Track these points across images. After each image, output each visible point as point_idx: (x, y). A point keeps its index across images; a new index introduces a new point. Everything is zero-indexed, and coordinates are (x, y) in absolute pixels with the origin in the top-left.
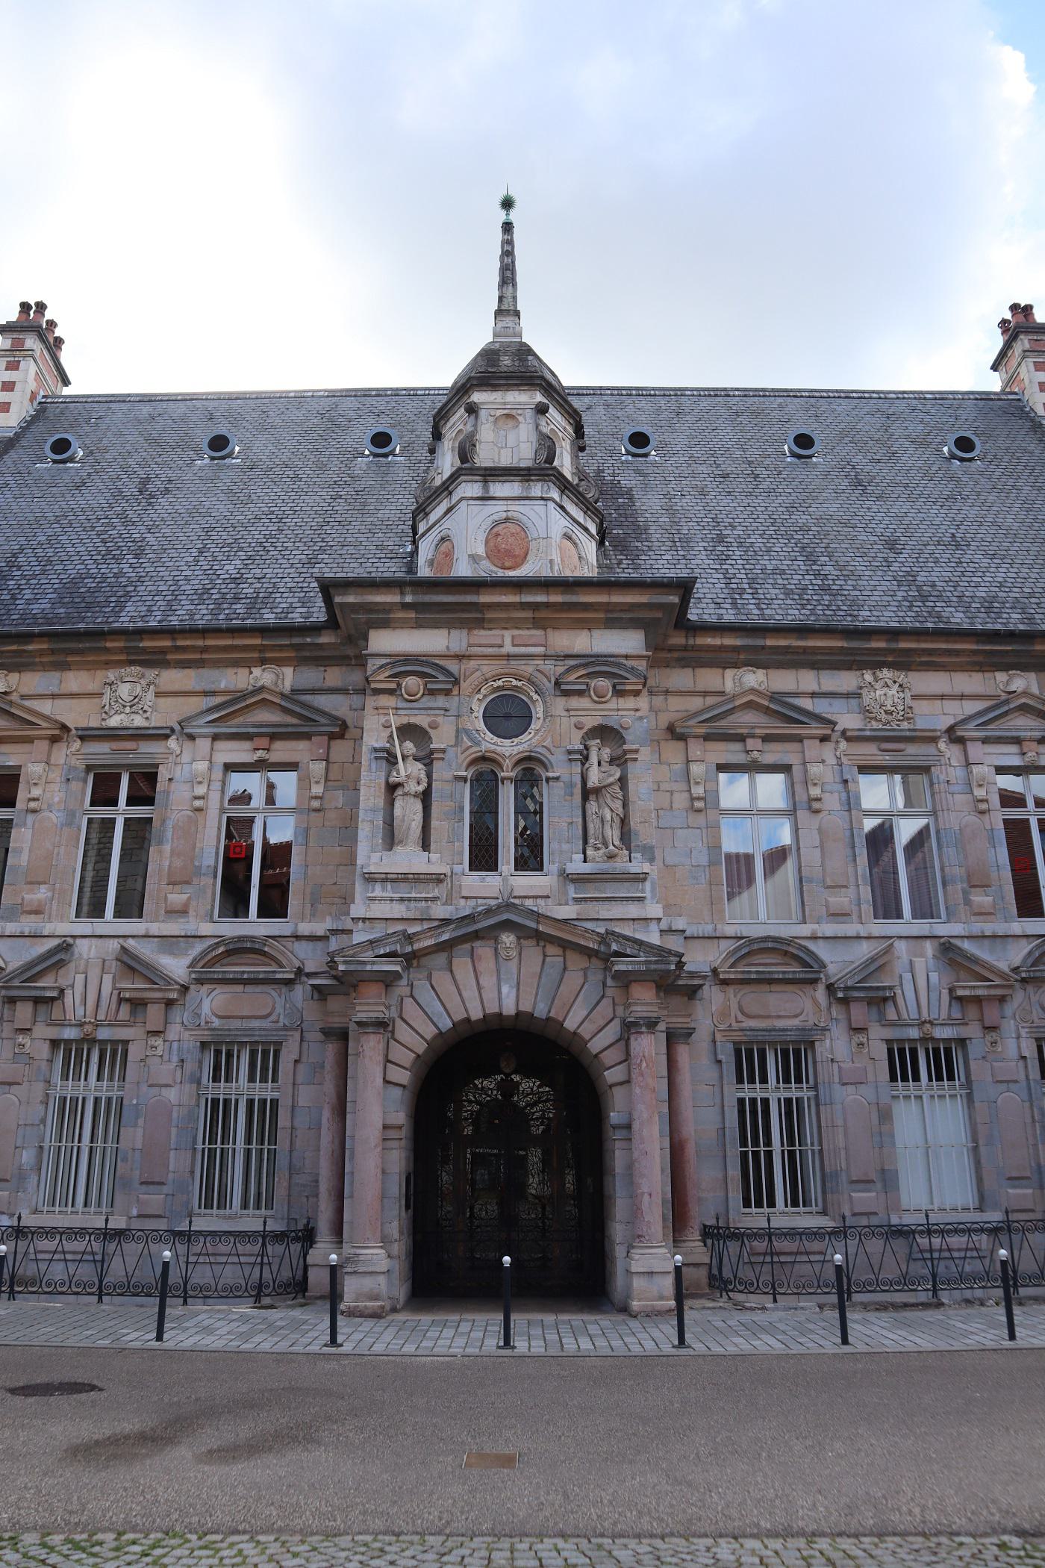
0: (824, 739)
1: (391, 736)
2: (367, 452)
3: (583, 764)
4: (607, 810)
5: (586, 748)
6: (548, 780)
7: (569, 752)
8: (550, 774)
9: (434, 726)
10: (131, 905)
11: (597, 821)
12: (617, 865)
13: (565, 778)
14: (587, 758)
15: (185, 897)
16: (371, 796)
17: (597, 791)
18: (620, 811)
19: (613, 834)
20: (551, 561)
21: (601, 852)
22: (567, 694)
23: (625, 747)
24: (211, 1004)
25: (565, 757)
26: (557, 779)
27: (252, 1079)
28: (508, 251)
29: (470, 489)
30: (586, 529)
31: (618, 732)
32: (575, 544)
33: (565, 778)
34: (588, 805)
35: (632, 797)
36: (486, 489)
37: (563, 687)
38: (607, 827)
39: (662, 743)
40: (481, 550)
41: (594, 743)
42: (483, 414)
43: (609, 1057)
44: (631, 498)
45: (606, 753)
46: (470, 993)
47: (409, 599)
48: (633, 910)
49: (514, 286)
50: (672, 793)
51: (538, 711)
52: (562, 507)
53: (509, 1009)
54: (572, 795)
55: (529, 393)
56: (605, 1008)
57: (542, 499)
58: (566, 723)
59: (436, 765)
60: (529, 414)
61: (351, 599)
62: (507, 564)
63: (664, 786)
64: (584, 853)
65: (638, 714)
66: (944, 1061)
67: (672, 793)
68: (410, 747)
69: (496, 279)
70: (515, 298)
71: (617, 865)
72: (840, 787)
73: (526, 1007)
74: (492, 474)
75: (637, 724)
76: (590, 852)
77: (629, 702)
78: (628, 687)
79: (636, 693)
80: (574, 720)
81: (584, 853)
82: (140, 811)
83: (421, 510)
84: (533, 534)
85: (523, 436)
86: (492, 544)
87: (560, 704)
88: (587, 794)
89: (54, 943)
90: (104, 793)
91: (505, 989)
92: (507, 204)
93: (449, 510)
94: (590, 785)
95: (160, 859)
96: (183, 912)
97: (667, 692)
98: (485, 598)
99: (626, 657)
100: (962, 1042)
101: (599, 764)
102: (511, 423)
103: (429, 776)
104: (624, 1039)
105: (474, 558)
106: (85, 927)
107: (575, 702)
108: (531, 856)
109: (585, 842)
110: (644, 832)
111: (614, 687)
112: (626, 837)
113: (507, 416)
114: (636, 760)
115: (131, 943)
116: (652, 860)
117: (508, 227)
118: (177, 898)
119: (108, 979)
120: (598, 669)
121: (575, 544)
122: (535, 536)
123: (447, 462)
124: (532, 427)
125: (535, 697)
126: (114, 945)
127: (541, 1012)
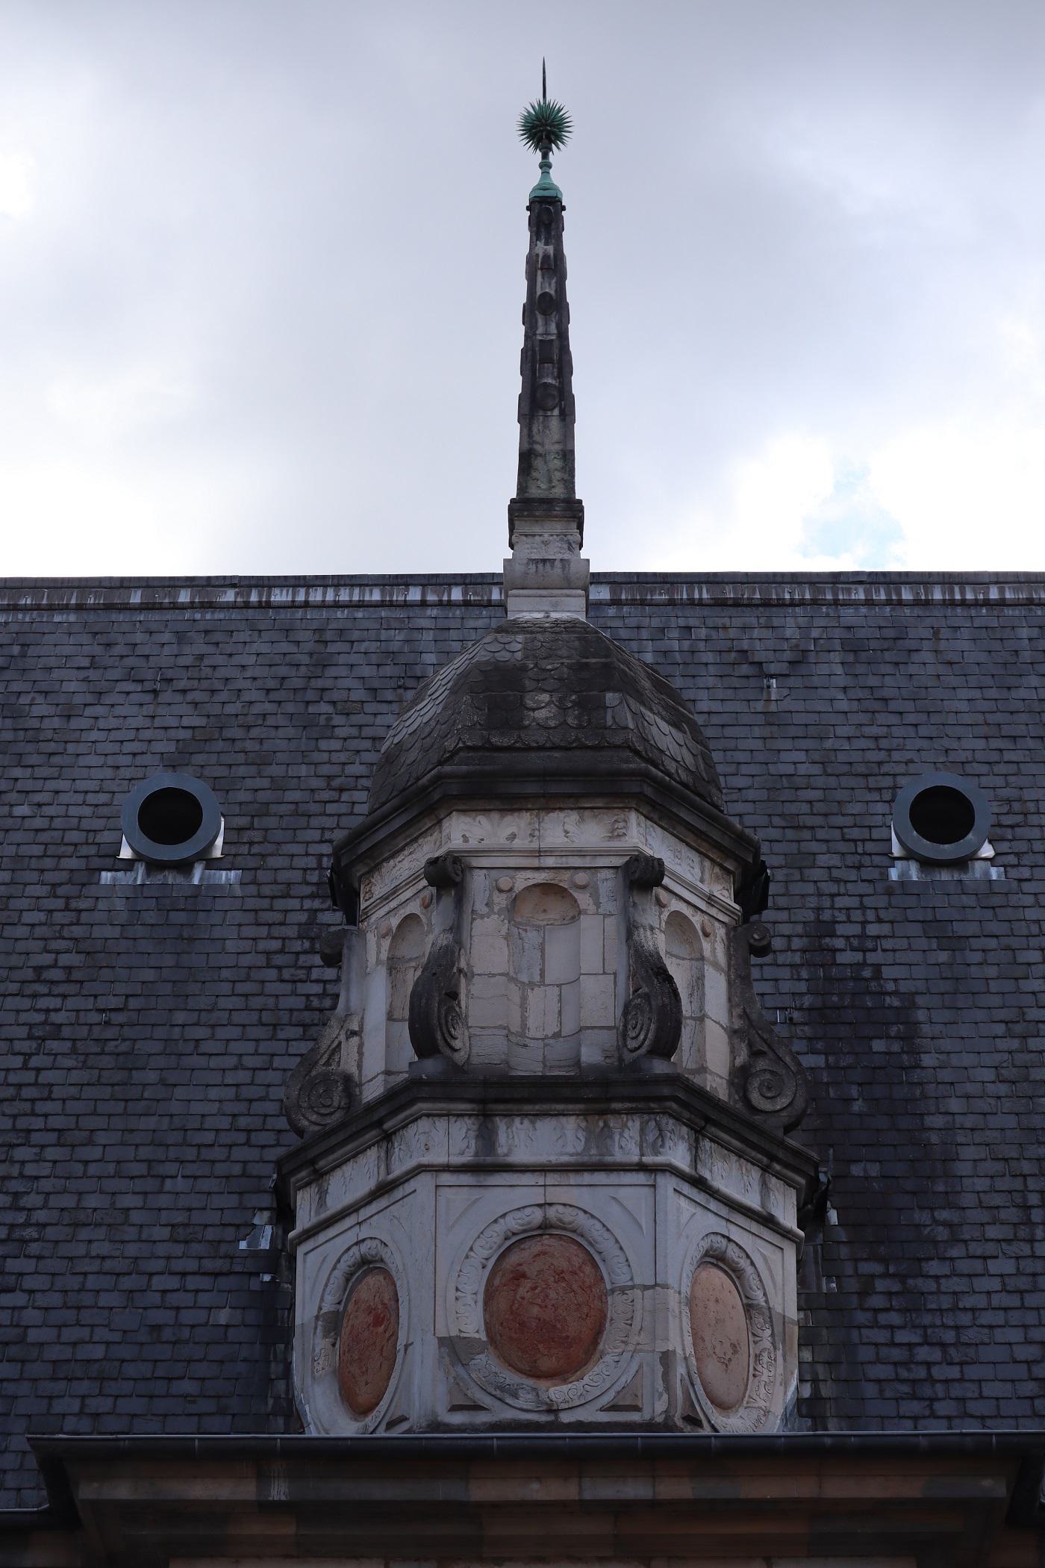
2: (126, 853)
20: (666, 1358)
28: (546, 306)
29: (442, 1138)
30: (768, 1221)
32: (735, 1273)
36: (487, 1138)
40: (472, 1323)
42: (478, 884)
44: (910, 1036)
47: (279, 1491)
49: (567, 415)
52: (699, 1183)
55: (608, 818)
57: (641, 1167)
60: (607, 884)
61: (123, 1491)
62: (546, 1363)
69: (509, 384)
70: (567, 457)
74: (498, 1095)
83: (309, 1160)
84: (616, 1273)
85: (591, 955)
92: (544, 129)
93: (384, 1189)
98: (484, 1490)
102: (556, 909)
105: (455, 1349)
113: (549, 889)
117: (546, 213)
121: (735, 1273)
122: (623, 1280)
123: (375, 1047)
124: (613, 926)
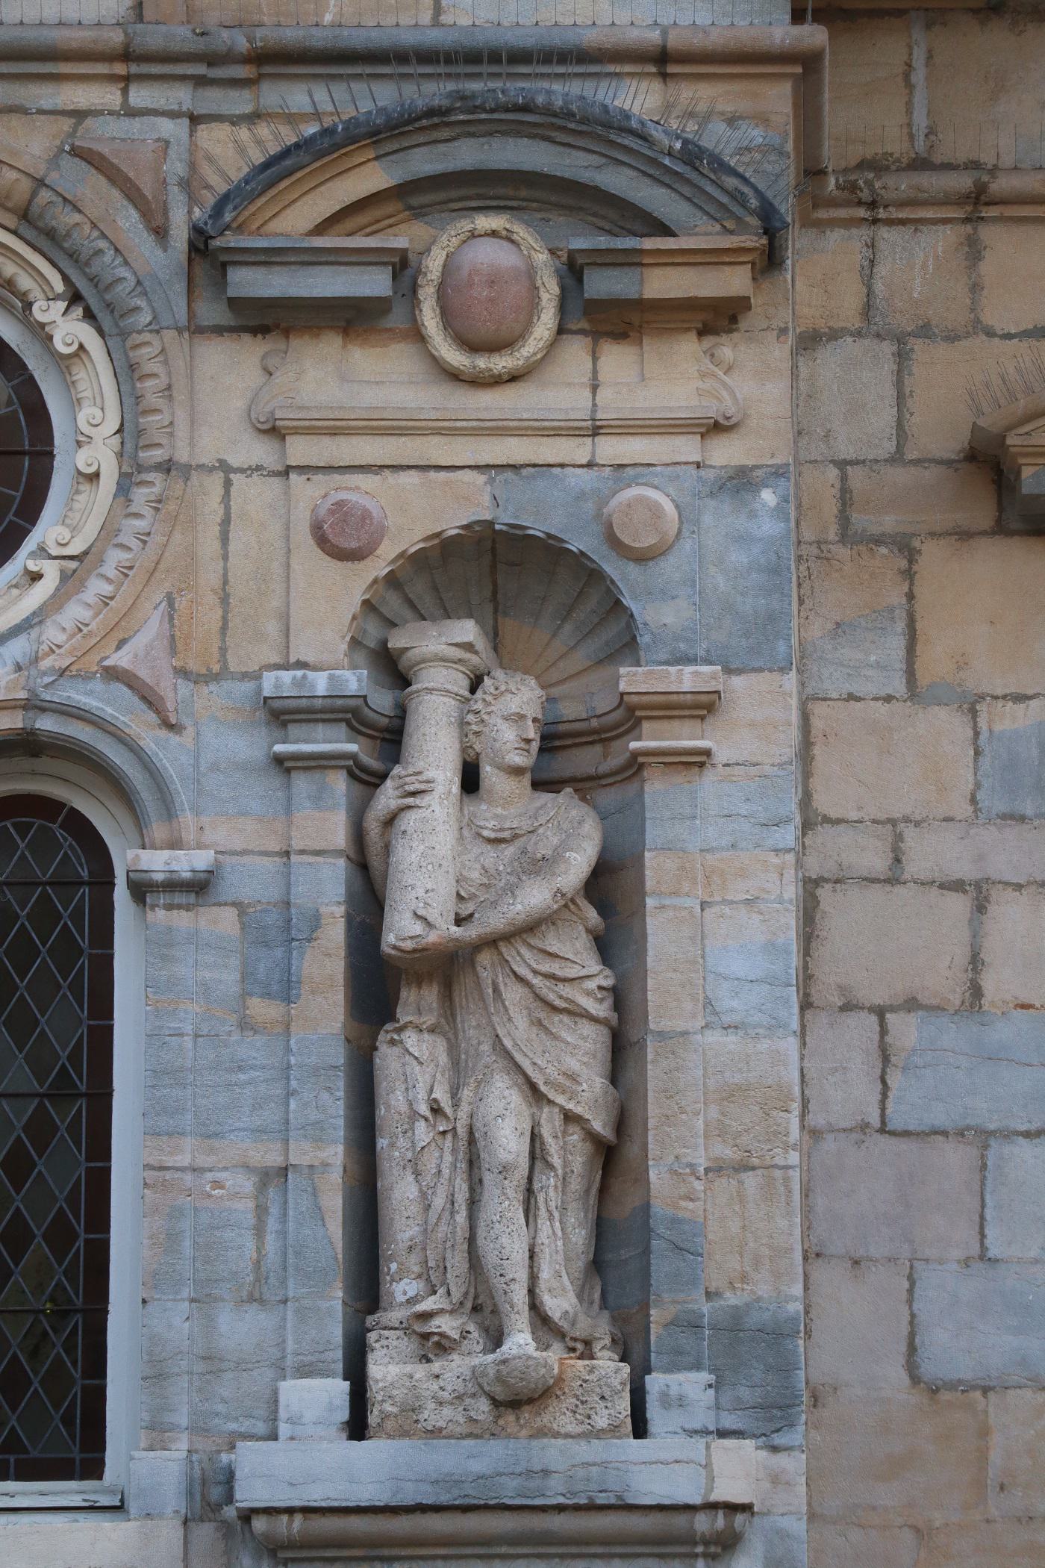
3: (368, 780)
4: (489, 1095)
5: (395, 671)
6: (141, 890)
7: (281, 715)
8: (157, 862)
11: (444, 1159)
12: (552, 1453)
13: (252, 881)
14: (392, 738)
17: (448, 967)
18: (590, 1093)
19: (539, 1249)
21: (455, 1368)
22: (269, 321)
23: (635, 679)
25: (249, 745)
26: (198, 888)
31: (590, 575)
33: (252, 881)
34: (388, 1059)
35: (665, 1004)
37: (248, 282)
38: (502, 1205)
39: (933, 556)
41: (442, 644)
45: (514, 709)
50: (979, 895)
51: (87, 425)
54: (287, 990)
58: (268, 517)
63: (933, 853)
64: (356, 1372)
65: (725, 453)
67: (979, 895)
71: (552, 1453)
75: (717, 520)
76: (385, 1369)
77: (664, 378)
78: (663, 284)
79: (718, 318)
80: (310, 496)
81: (356, 1372)
87: (225, 384)
88: (377, 985)
94: (402, 930)
97: (978, 203)
99: (662, 61)
101: (470, 781)
107: (325, 376)
109: (367, 1288)
110: (732, 1241)
111: (573, 270)
112: (619, 1249)
114: (697, 761)
116: (771, 1417)
120: (467, 154)
125: (69, 331)
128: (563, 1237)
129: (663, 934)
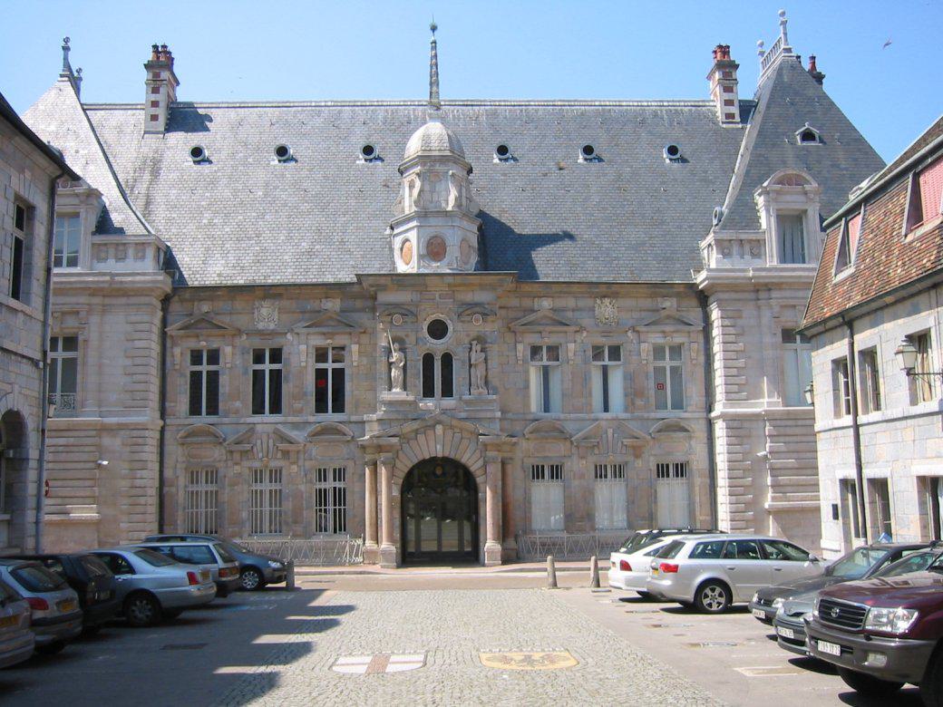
0: (576, 332)
1: (389, 343)
4: (478, 373)
5: (471, 344)
9: (407, 336)
10: (276, 408)
15: (300, 405)
16: (382, 368)
17: (476, 365)
19: (481, 382)
24: (315, 450)
27: (335, 480)
35: (489, 367)
43: (478, 473)
45: (479, 347)
46: (424, 448)
48: (489, 415)
53: (440, 455)
56: (478, 454)
59: (408, 354)
66: (619, 471)
68: (397, 346)
72: (582, 354)
73: (446, 454)
82: (276, 366)
86: (430, 248)
88: (470, 366)
89: (247, 428)
90: (259, 358)
91: (438, 447)
92: (434, 29)
95: (287, 389)
96: (300, 411)
100: (626, 463)
103: (406, 358)
104: (485, 466)
106: (257, 418)
108: (448, 391)
110: (494, 381)
112: (486, 383)
115: (280, 427)
118: (298, 405)
119: (271, 441)
126: (273, 427)
127: (452, 456)
128: (483, 381)
129: (489, 362)
